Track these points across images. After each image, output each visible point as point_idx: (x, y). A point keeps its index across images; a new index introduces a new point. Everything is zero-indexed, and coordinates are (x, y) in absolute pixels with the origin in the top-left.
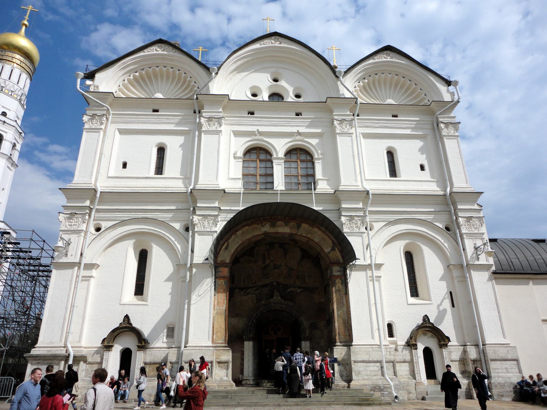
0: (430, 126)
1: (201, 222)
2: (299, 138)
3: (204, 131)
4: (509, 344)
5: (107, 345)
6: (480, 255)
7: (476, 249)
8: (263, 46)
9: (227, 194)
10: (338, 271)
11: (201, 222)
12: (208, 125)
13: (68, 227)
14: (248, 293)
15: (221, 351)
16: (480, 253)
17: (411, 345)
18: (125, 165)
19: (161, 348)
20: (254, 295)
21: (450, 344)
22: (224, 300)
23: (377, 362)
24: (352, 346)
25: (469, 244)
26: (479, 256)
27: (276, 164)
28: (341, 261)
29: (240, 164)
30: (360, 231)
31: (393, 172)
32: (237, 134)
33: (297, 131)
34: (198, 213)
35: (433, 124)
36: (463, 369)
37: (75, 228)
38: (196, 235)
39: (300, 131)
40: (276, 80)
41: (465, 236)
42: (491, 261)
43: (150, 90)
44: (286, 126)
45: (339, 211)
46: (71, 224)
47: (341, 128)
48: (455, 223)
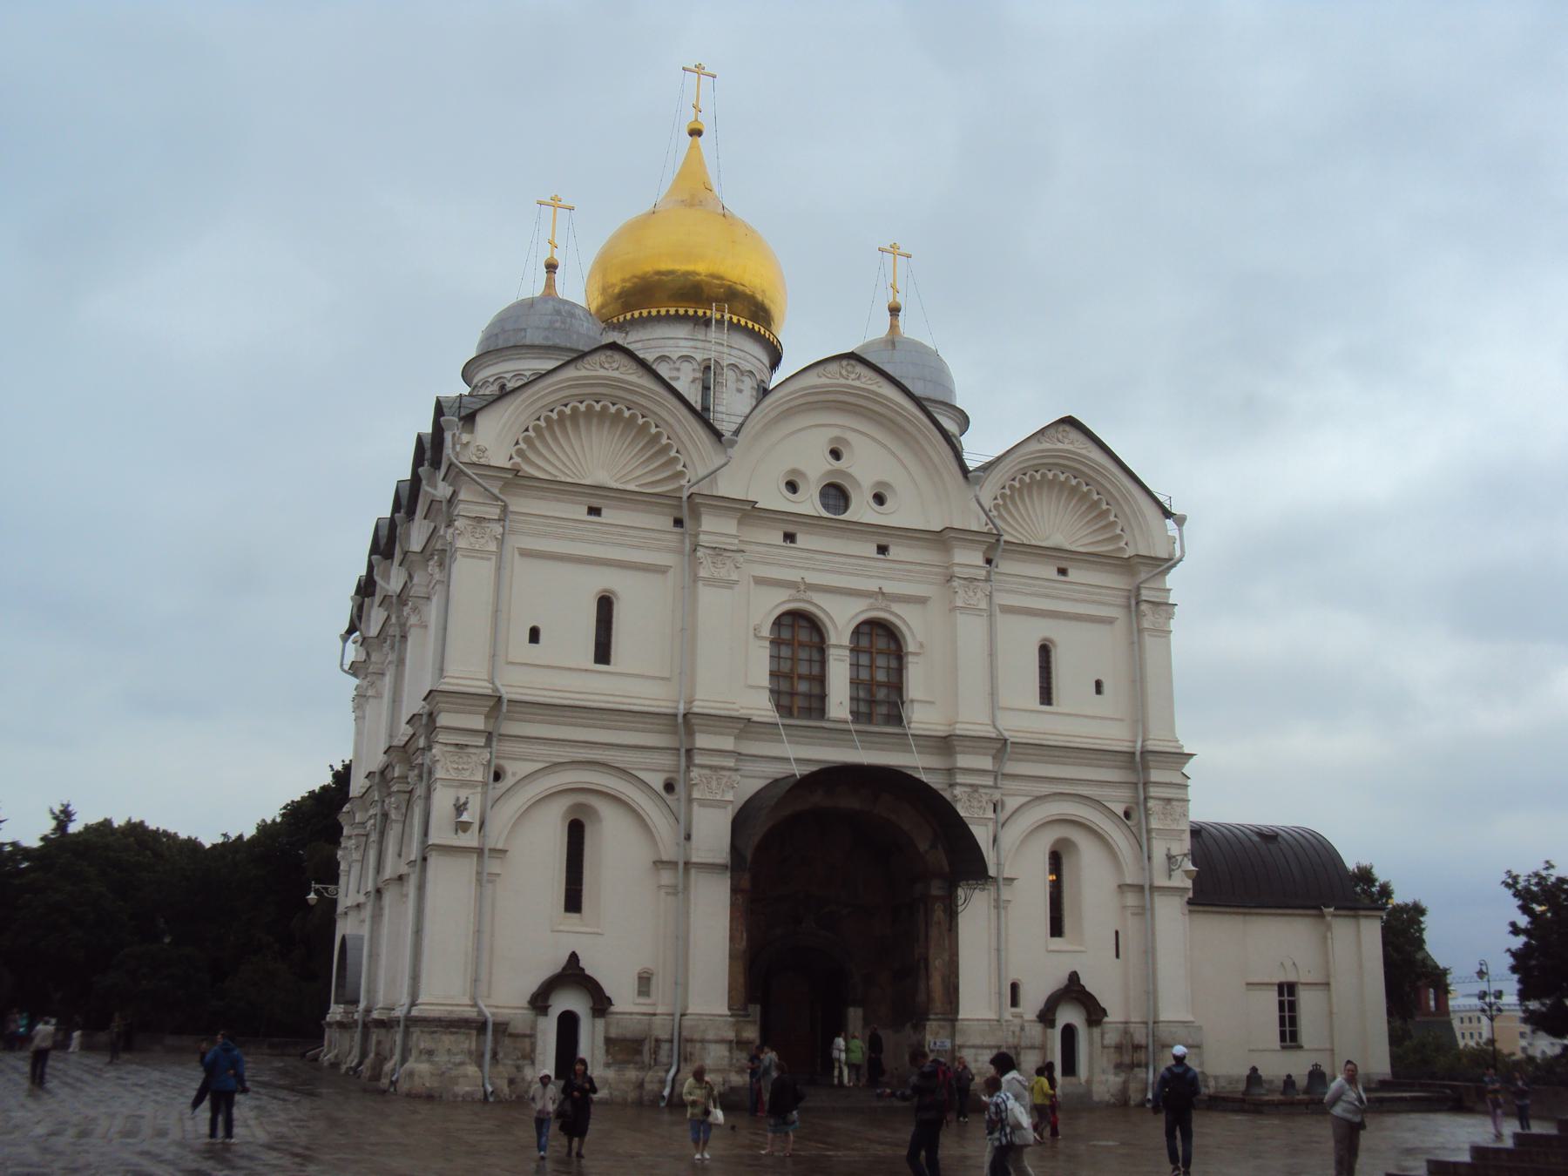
0: (1121, 601)
2: (881, 603)
3: (704, 579)
4: (1193, 1022)
5: (539, 1002)
6: (1173, 870)
7: (1170, 858)
8: (824, 380)
9: (751, 724)
11: (704, 779)
12: (711, 565)
13: (451, 771)
16: (1174, 868)
17: (1046, 1017)
18: (534, 635)
19: (631, 1014)
21: (1106, 1019)
22: (742, 932)
25: (1159, 849)
26: (1172, 873)
27: (835, 660)
28: (947, 869)
30: (985, 816)
32: (760, 581)
33: (878, 590)
34: (698, 760)
35: (1129, 598)
36: (1119, 1061)
37: (466, 776)
38: (695, 806)
39: (885, 590)
40: (836, 454)
41: (1154, 834)
42: (1189, 884)
44: (858, 575)
45: (951, 772)
46: (456, 766)
47: (967, 597)
48: (1142, 808)
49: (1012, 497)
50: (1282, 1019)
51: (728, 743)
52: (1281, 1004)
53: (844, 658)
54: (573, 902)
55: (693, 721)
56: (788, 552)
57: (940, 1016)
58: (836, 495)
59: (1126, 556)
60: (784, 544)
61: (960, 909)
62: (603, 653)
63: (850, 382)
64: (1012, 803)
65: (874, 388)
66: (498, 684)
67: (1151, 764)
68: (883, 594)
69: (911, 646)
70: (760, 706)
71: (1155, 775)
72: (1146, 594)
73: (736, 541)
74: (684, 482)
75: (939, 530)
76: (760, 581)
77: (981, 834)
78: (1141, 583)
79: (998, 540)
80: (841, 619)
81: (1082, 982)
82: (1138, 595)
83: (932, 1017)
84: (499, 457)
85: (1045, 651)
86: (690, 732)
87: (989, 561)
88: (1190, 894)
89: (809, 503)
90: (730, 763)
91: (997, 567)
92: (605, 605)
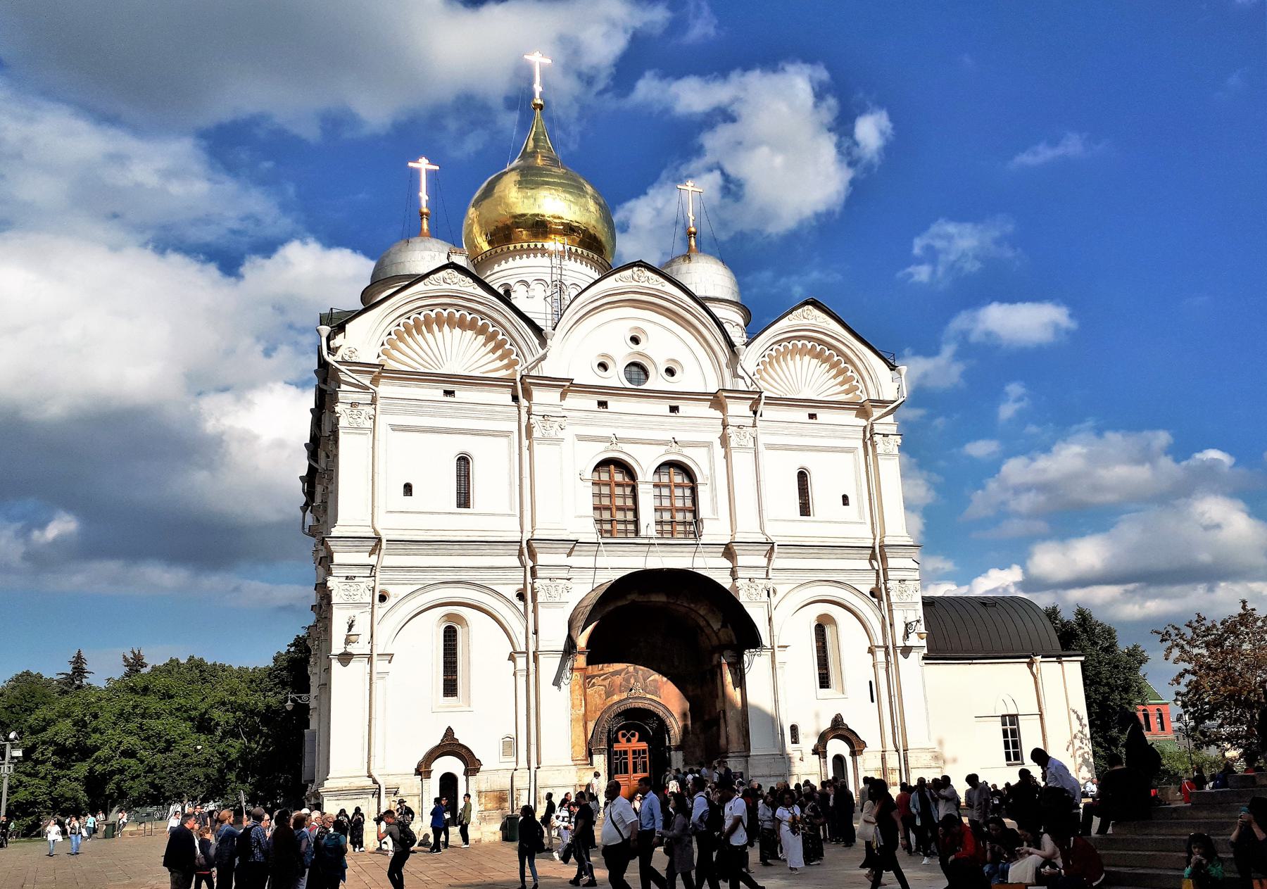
1: (546, 588)
2: (675, 448)
3: (538, 439)
6: (910, 633)
10: (732, 656)
14: (594, 685)
15: (584, 771)
16: (911, 631)
20: (602, 687)
23: (780, 776)
24: (749, 756)
27: (642, 492)
29: (587, 491)
30: (761, 600)
31: (805, 510)
32: (581, 438)
40: (635, 340)
42: (924, 643)
43: (425, 339)
47: (738, 439)
49: (770, 363)
50: (1006, 745)
51: (561, 559)
52: (1005, 733)
53: (648, 491)
54: (450, 688)
55: (534, 545)
56: (602, 415)
57: (737, 754)
58: (638, 370)
59: (861, 401)
60: (599, 410)
61: (746, 671)
62: (464, 500)
63: (641, 284)
64: (781, 590)
65: (659, 287)
66: (378, 528)
67: (888, 555)
68: (676, 442)
69: (700, 480)
70: (588, 531)
71: (892, 563)
72: (877, 428)
73: (560, 409)
74: (516, 368)
75: (715, 392)
76: (581, 438)
77: (757, 614)
78: (875, 420)
79: (760, 396)
80: (645, 462)
81: (845, 722)
82: (872, 429)
83: (730, 755)
84: (368, 355)
85: (802, 477)
86: (533, 555)
87: (755, 413)
88: (925, 651)
89: (615, 376)
90: (564, 574)
91: (761, 416)
92: (464, 462)
